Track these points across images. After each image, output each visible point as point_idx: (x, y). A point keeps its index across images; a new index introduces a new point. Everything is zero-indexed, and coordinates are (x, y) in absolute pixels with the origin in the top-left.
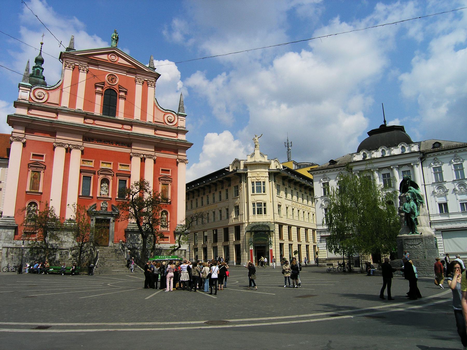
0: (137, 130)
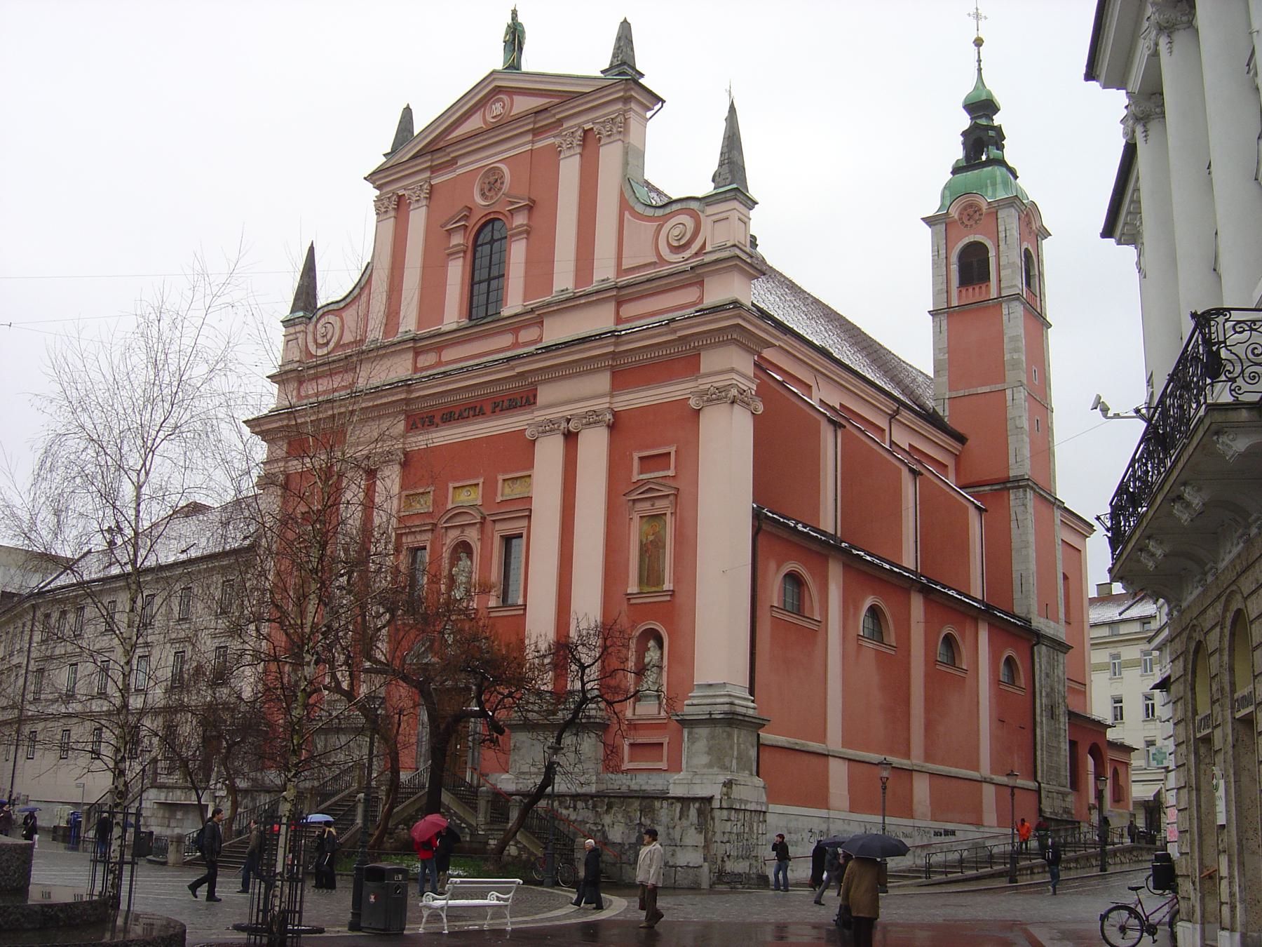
0: (558, 330)
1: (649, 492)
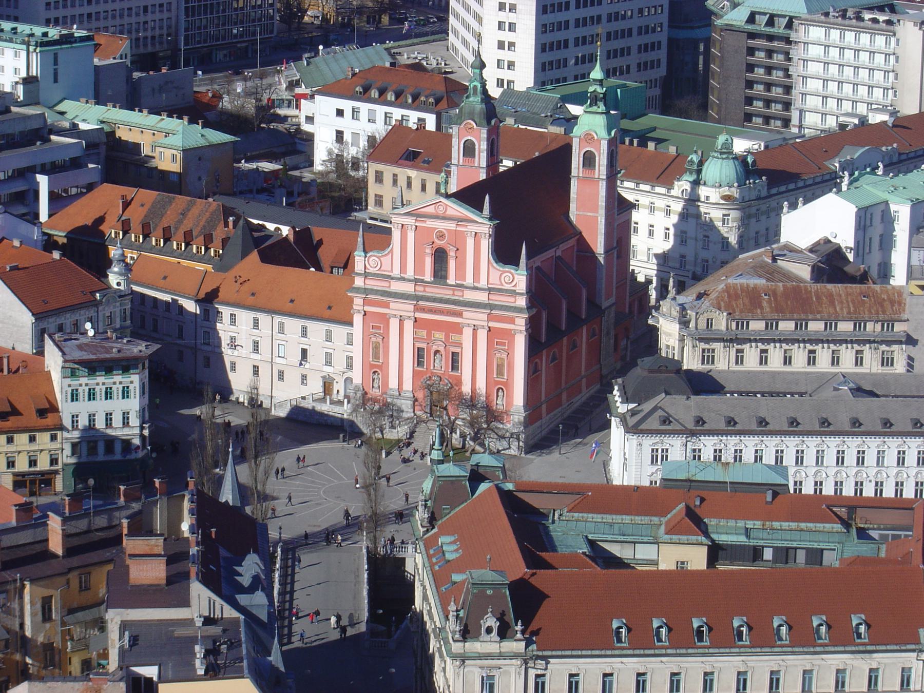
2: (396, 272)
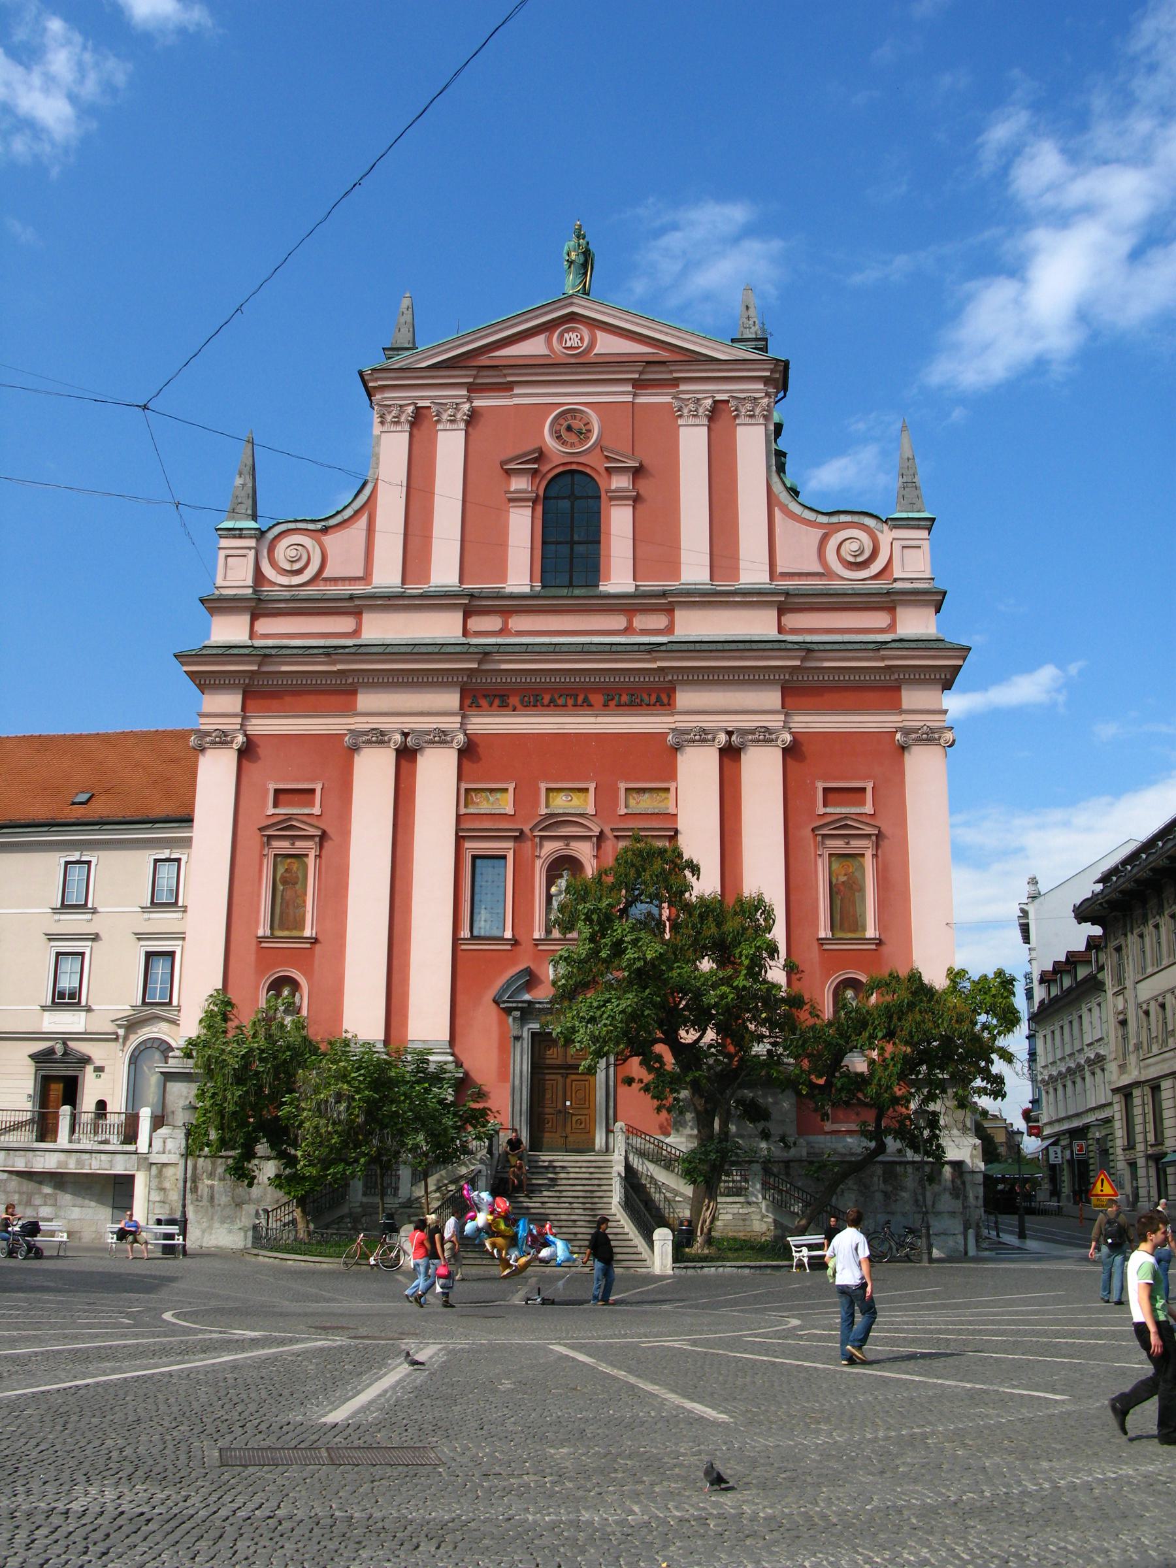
0: (693, 625)
1: (843, 827)
2: (387, 575)
